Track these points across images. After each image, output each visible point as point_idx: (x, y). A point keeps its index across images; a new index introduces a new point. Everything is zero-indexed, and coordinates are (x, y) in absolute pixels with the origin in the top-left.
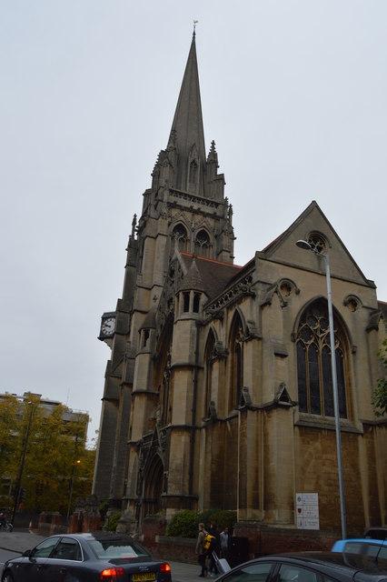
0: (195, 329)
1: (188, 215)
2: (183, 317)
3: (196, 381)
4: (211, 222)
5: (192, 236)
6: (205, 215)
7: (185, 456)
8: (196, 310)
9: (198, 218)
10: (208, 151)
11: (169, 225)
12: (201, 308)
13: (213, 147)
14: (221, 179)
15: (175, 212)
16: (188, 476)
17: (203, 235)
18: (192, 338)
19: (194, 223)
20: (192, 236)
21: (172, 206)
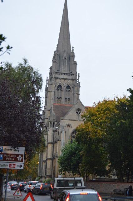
0: (53, 132)
1: (63, 81)
2: (50, 129)
3: (53, 147)
4: (71, 82)
5: (64, 89)
6: (69, 80)
7: (50, 166)
8: (53, 127)
9: (67, 81)
10: (72, 48)
11: (55, 86)
12: (55, 126)
13: (73, 49)
14: (75, 64)
15: (58, 81)
16: (51, 171)
17: (68, 87)
18: (52, 135)
19: (64, 84)
20: (64, 89)
21: (56, 78)
